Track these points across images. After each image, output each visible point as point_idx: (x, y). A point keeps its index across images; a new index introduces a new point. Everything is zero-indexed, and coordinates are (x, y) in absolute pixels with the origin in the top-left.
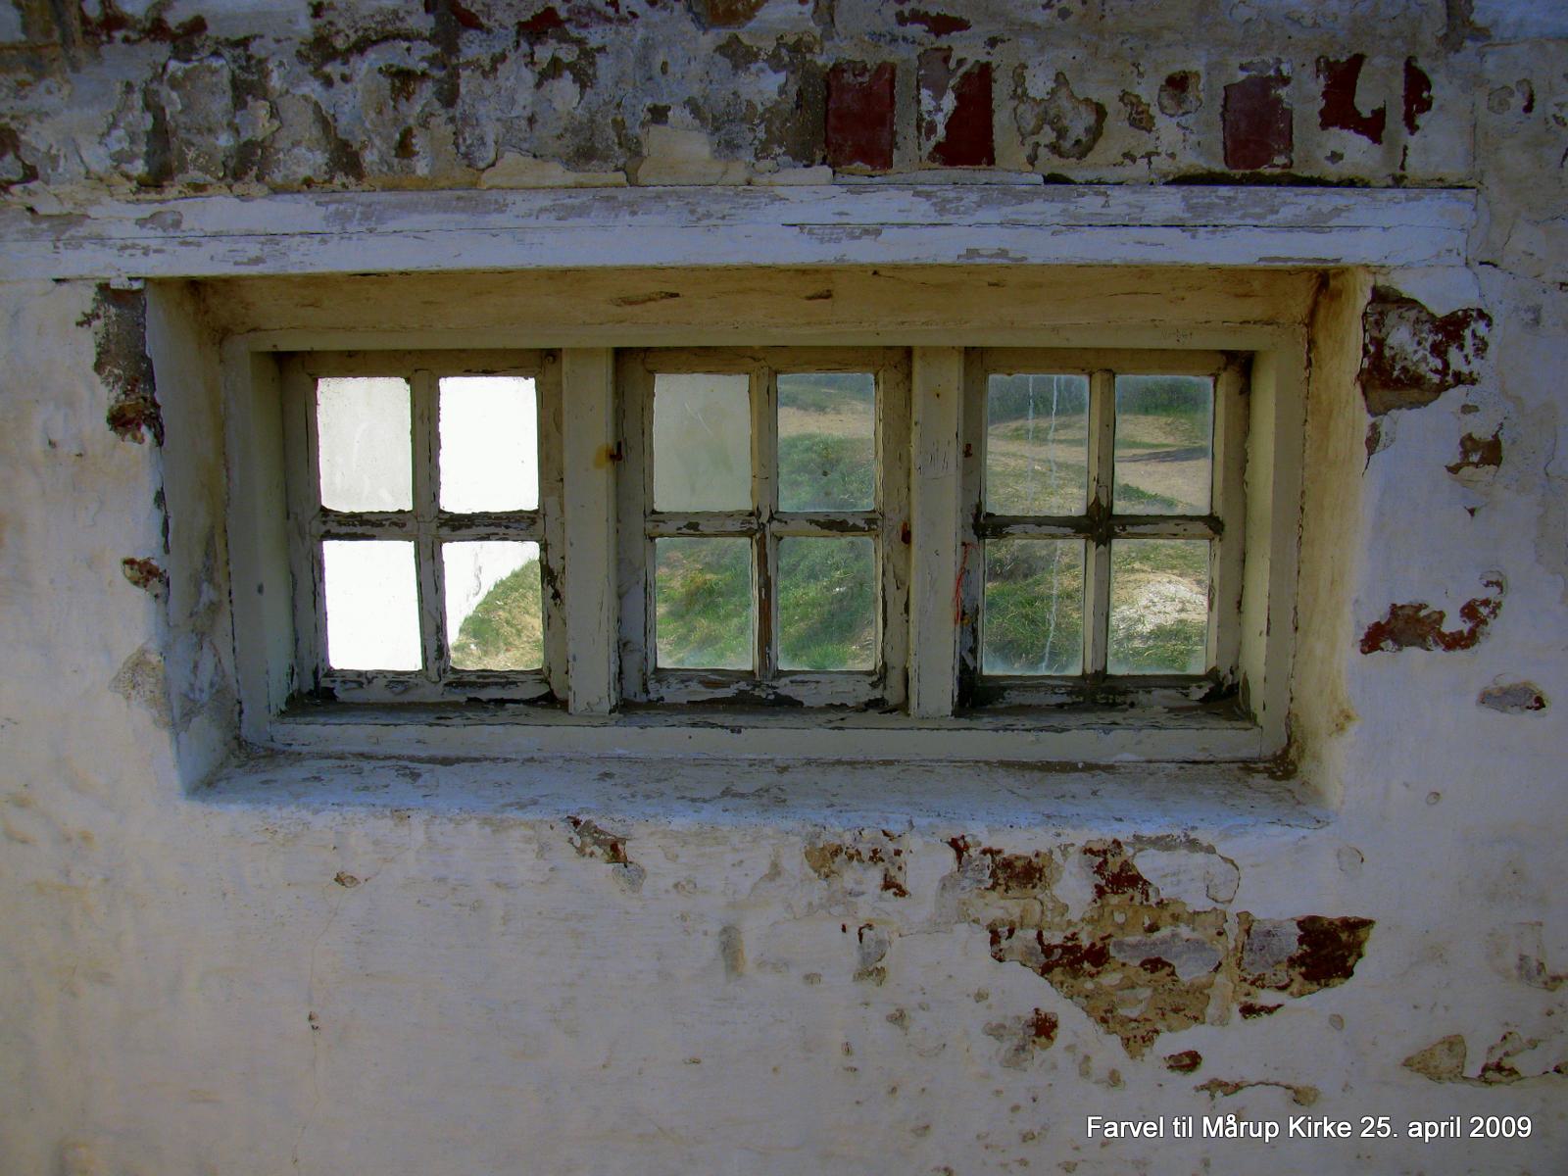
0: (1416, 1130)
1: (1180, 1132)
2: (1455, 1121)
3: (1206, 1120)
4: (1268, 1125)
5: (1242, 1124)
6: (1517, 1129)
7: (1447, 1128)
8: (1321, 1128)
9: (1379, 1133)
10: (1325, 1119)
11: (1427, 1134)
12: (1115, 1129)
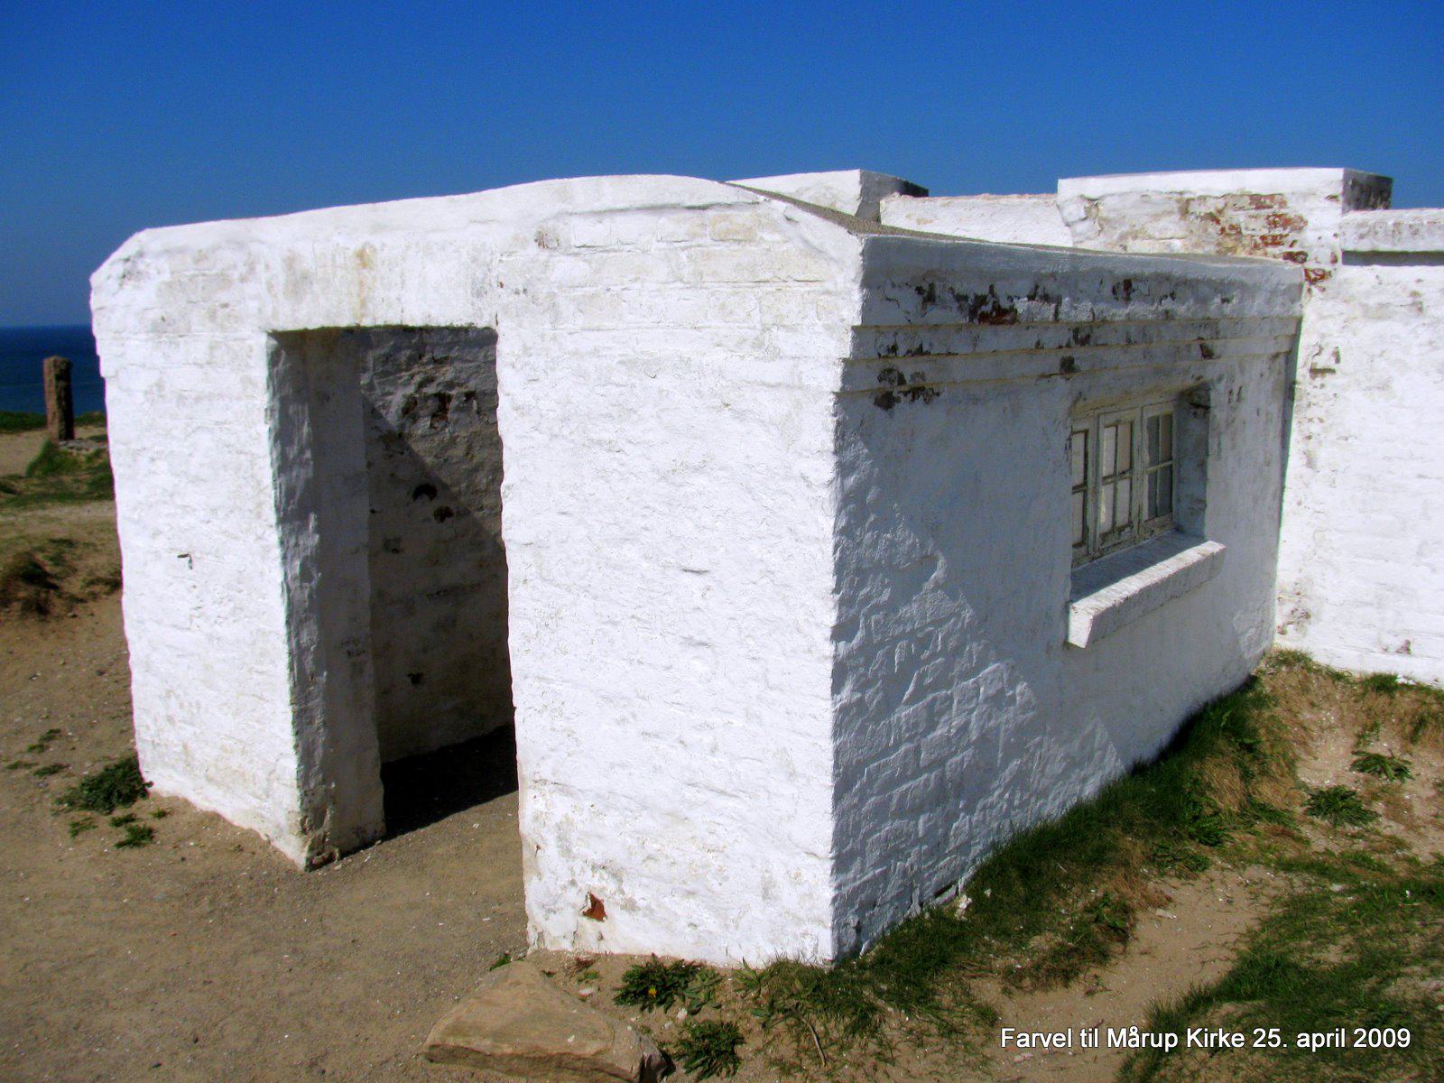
0: (1304, 1040)
1: (1087, 1043)
2: (1340, 1032)
3: (1111, 1032)
4: (1168, 1036)
5: (1144, 1036)
6: (1397, 1040)
7: (1333, 1040)
8: (1216, 1040)
9: (1270, 1043)
10: (1221, 1030)
11: (1315, 1045)
12: (1027, 1039)
